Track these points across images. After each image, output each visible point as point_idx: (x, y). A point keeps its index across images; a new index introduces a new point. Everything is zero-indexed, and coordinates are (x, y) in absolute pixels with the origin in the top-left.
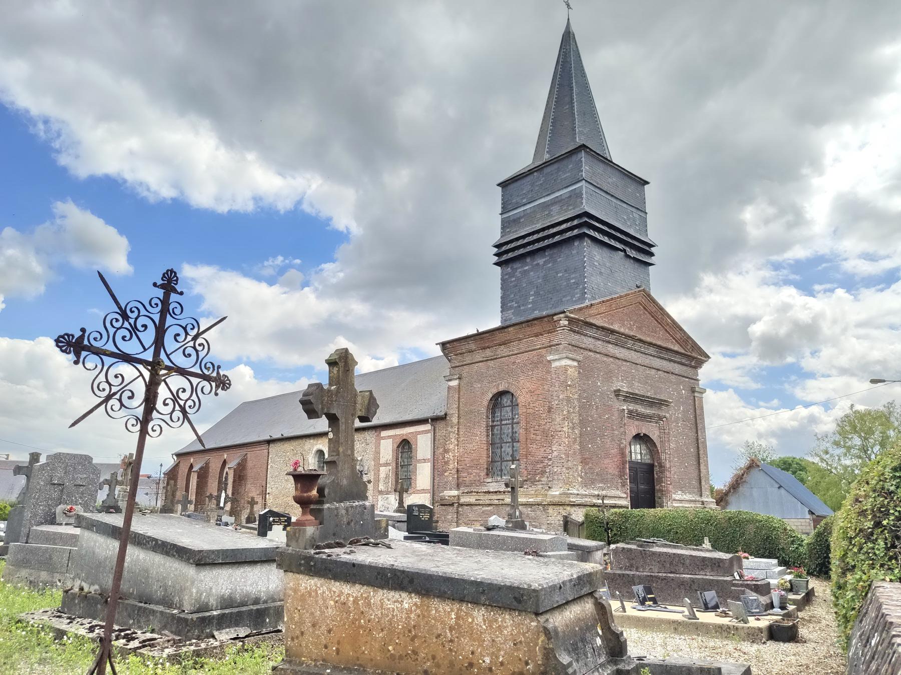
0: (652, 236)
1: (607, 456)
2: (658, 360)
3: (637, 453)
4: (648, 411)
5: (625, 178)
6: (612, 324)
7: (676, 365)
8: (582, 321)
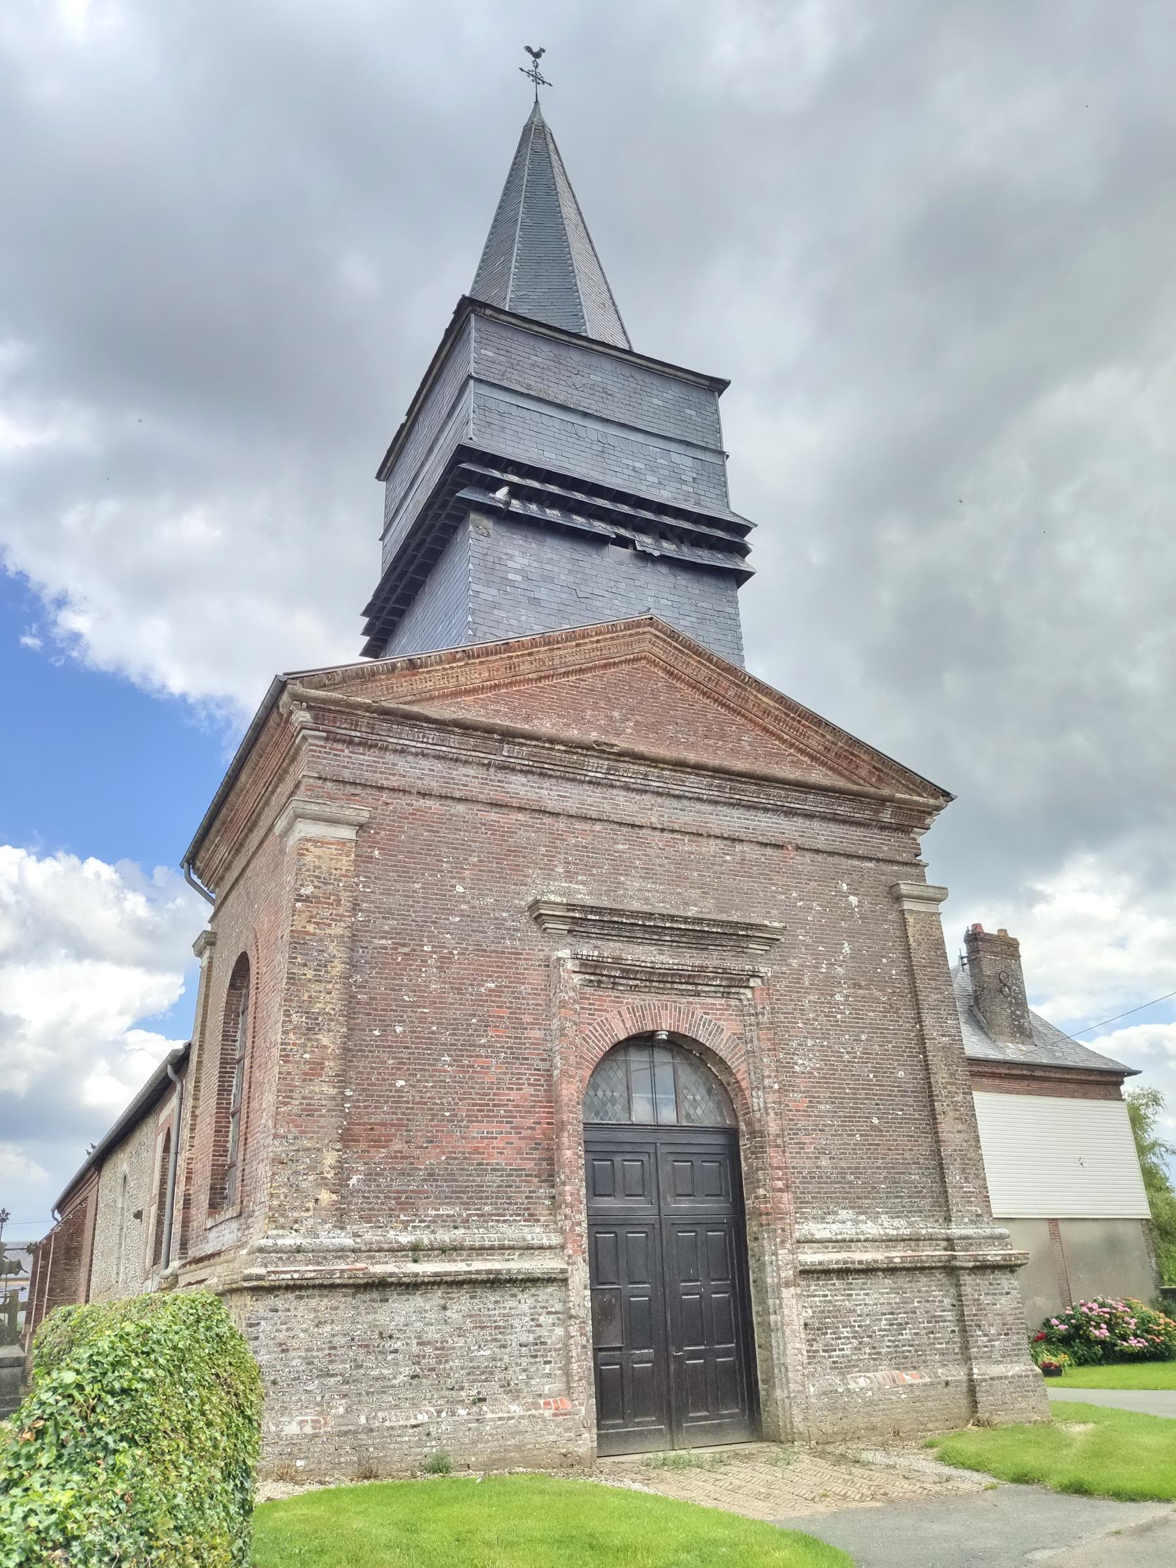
0: (739, 507)
1: (485, 1110)
2: (736, 812)
3: (656, 1100)
4: (689, 960)
5: (638, 376)
6: (528, 718)
7: (816, 824)
8: (368, 708)
